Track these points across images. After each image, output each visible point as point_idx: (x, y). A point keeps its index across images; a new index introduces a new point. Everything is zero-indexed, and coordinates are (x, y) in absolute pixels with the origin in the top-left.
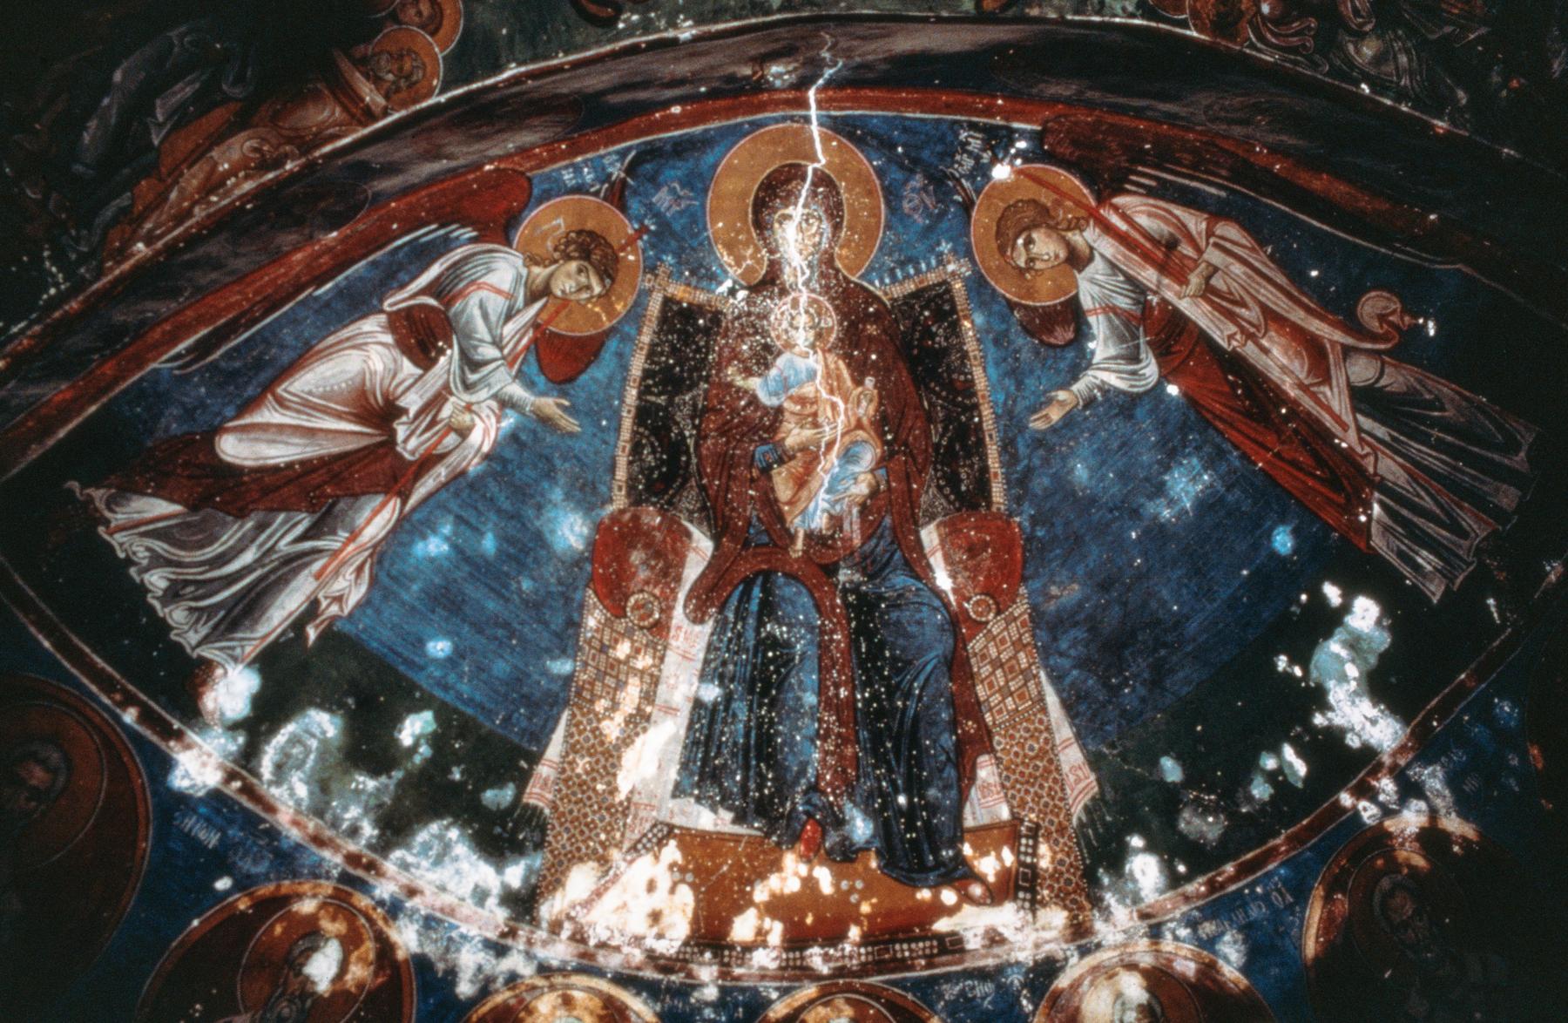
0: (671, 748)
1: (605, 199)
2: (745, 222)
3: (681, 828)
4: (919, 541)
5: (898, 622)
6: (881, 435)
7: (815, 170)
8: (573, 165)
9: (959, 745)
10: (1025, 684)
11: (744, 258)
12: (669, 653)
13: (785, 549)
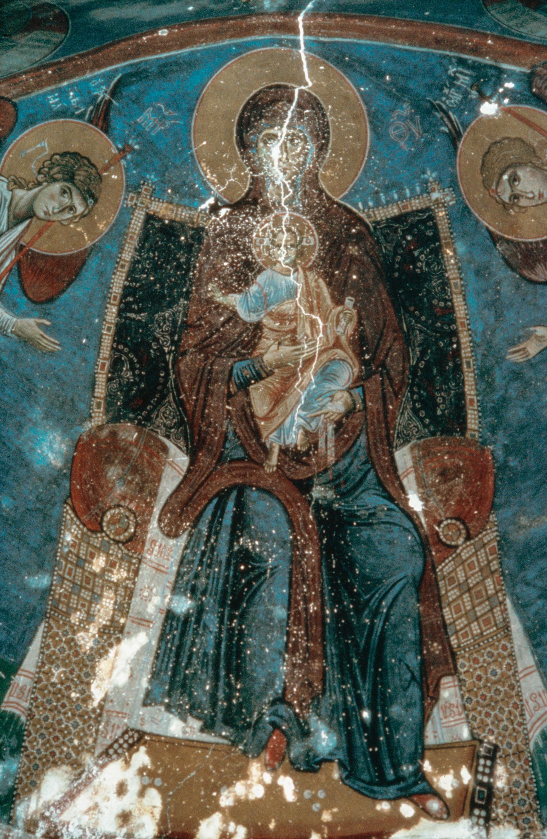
0: (143, 658)
1: (90, 121)
2: (229, 141)
3: (150, 734)
4: (392, 460)
5: (369, 542)
6: (360, 354)
7: (301, 92)
8: (59, 90)
9: (423, 664)
10: (491, 610)
11: (228, 176)
12: (143, 566)
13: (261, 465)
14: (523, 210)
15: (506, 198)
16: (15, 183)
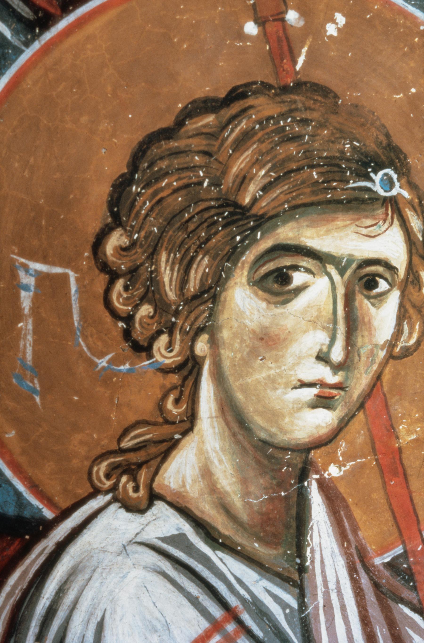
16: (131, 470)
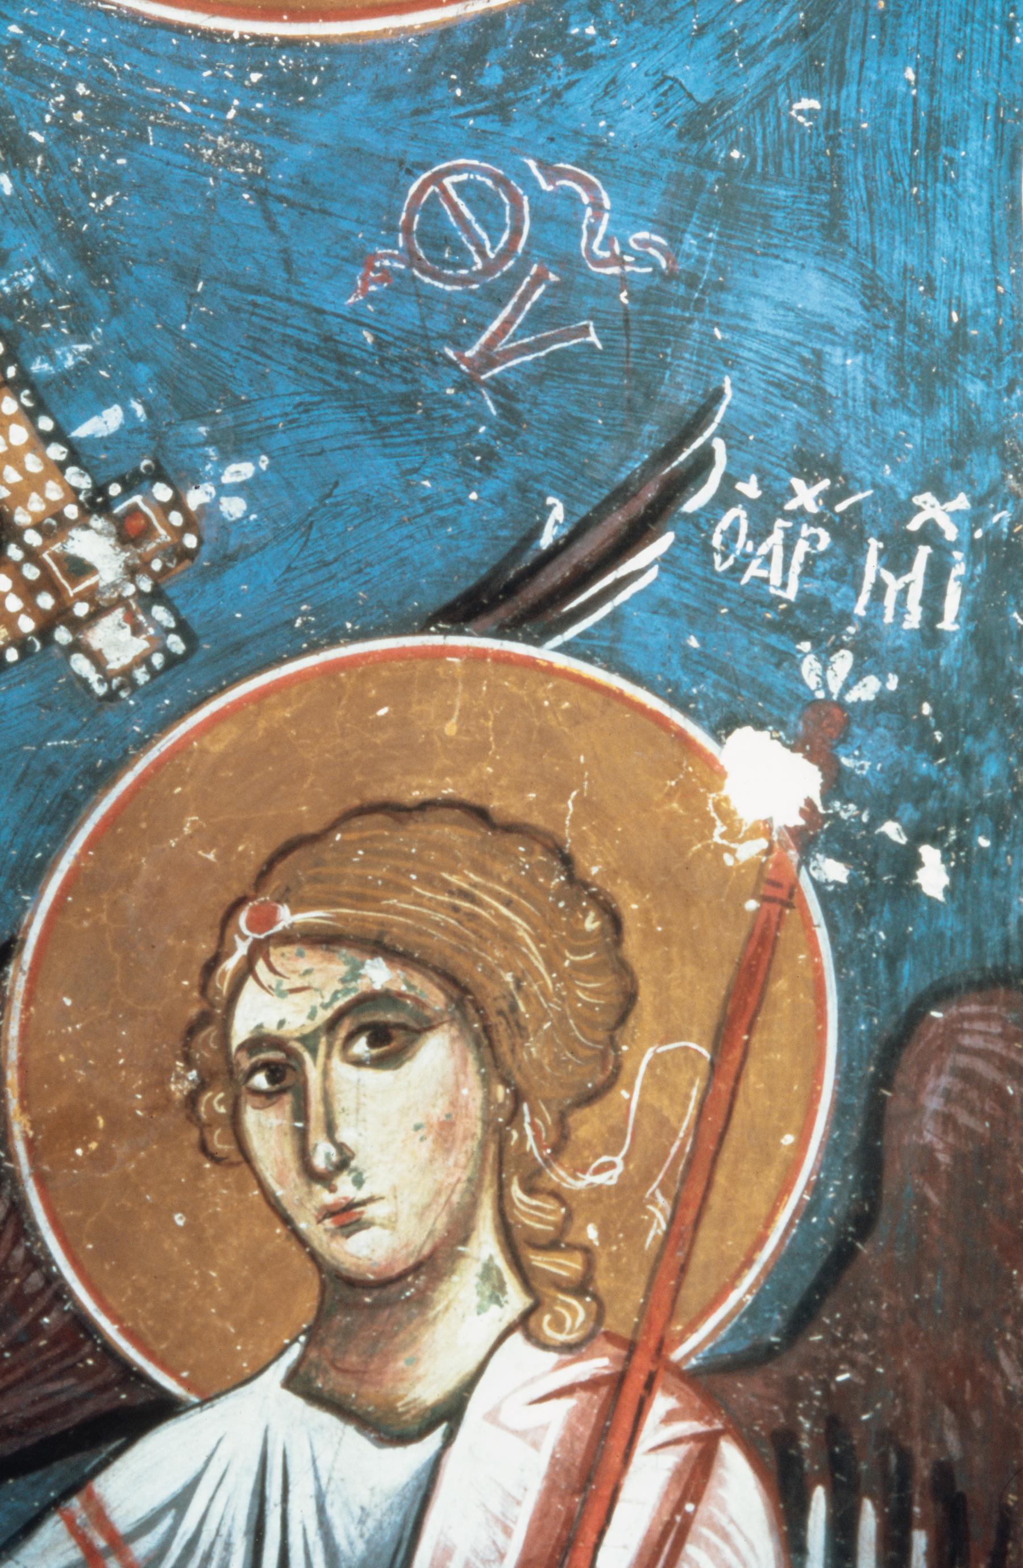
14: (219, 1143)
15: (256, 1012)
